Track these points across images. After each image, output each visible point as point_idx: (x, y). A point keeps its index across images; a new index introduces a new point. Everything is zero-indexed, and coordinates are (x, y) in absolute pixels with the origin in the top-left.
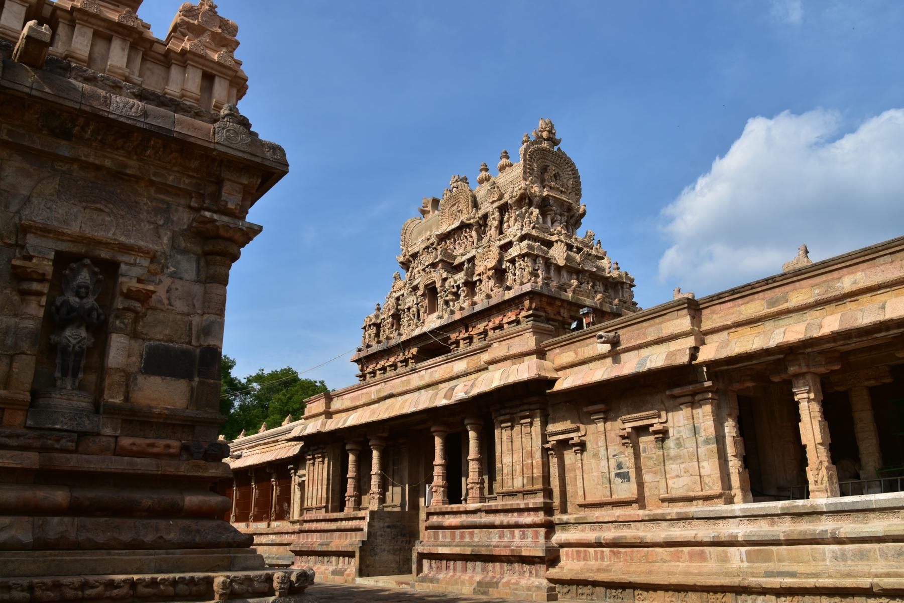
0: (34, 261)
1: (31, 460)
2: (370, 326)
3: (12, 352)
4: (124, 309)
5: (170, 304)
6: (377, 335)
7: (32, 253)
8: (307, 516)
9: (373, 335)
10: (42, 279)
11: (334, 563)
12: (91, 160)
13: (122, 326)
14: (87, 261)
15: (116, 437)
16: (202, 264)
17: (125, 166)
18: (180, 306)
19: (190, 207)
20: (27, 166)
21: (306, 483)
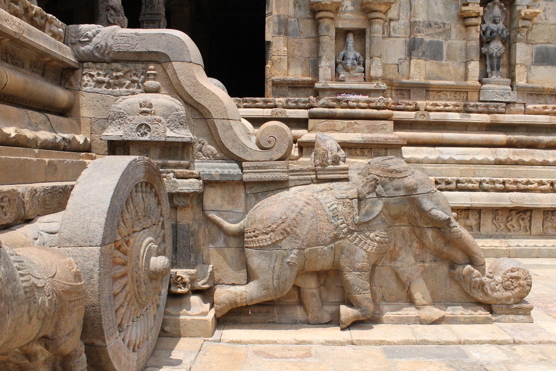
0: (470, 5)
1: (485, 118)
3: (465, 61)
4: (522, 27)
7: (468, 1)
13: (522, 37)
15: (524, 104)
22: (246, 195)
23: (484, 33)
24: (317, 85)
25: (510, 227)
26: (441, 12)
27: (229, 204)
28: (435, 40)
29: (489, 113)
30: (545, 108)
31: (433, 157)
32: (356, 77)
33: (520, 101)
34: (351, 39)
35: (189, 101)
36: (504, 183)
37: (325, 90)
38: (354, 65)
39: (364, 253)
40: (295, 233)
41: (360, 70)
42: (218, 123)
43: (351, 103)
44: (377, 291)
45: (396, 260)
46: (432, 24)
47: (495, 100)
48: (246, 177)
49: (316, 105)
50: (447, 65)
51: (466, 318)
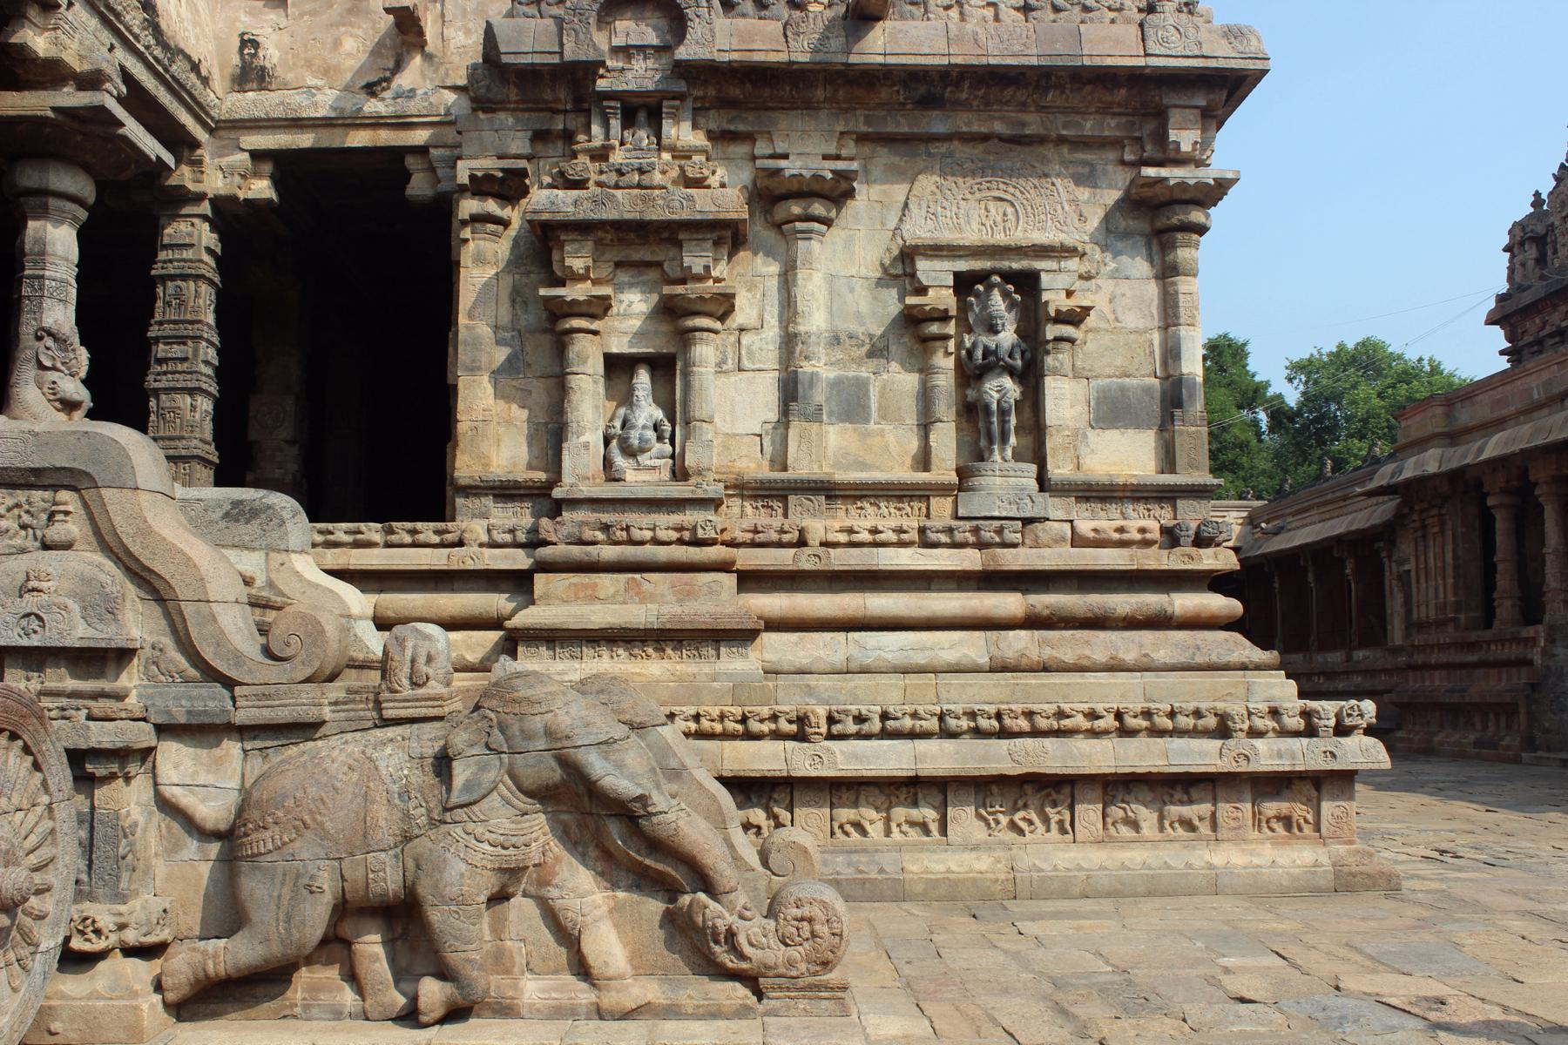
0: (931, 292)
1: (970, 560)
2: (1521, 244)
4: (1058, 339)
5: (1117, 320)
6: (1541, 261)
8: (1418, 639)
9: (1531, 263)
10: (944, 317)
11: (1478, 726)
12: (975, 128)
14: (996, 279)
16: (1155, 248)
17: (1023, 125)
18: (1132, 320)
19: (1123, 163)
20: (896, 159)
21: (1413, 574)
22: (245, 751)
23: (970, 353)
24: (557, 493)
25: (1023, 825)
26: (864, 306)
27: (208, 771)
28: (851, 374)
29: (981, 545)
30: (1121, 530)
31: (838, 659)
32: (654, 468)
33: (1061, 515)
34: (643, 378)
35: (134, 566)
36: (999, 716)
37: (574, 503)
38: (647, 441)
39: (463, 867)
40: (322, 825)
41: (661, 451)
42: (188, 610)
43: (637, 534)
44: (515, 952)
45: (548, 884)
46: (843, 337)
47: (996, 514)
48: (240, 717)
49: (554, 539)
50: (882, 433)
51: (699, 1007)
